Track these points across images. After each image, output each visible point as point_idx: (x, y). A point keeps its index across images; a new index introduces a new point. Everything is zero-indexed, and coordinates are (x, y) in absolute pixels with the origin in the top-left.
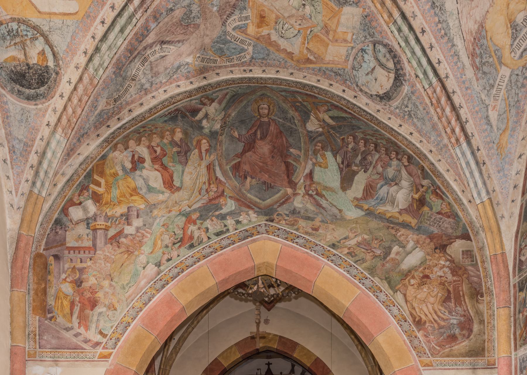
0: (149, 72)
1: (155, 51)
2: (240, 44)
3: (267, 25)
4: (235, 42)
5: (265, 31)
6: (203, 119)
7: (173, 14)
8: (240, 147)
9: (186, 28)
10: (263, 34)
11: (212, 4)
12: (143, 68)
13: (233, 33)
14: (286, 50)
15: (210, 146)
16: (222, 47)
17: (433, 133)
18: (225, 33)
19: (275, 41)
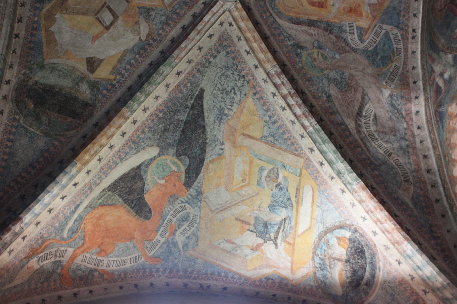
0: (388, 136)
1: (365, 123)
2: (379, 38)
3: (359, 6)
4: (377, 42)
5: (366, 10)
7: (333, 97)
9: (350, 88)
10: (369, 11)
11: (332, 58)
12: (380, 141)
13: (366, 43)
18: (364, 51)
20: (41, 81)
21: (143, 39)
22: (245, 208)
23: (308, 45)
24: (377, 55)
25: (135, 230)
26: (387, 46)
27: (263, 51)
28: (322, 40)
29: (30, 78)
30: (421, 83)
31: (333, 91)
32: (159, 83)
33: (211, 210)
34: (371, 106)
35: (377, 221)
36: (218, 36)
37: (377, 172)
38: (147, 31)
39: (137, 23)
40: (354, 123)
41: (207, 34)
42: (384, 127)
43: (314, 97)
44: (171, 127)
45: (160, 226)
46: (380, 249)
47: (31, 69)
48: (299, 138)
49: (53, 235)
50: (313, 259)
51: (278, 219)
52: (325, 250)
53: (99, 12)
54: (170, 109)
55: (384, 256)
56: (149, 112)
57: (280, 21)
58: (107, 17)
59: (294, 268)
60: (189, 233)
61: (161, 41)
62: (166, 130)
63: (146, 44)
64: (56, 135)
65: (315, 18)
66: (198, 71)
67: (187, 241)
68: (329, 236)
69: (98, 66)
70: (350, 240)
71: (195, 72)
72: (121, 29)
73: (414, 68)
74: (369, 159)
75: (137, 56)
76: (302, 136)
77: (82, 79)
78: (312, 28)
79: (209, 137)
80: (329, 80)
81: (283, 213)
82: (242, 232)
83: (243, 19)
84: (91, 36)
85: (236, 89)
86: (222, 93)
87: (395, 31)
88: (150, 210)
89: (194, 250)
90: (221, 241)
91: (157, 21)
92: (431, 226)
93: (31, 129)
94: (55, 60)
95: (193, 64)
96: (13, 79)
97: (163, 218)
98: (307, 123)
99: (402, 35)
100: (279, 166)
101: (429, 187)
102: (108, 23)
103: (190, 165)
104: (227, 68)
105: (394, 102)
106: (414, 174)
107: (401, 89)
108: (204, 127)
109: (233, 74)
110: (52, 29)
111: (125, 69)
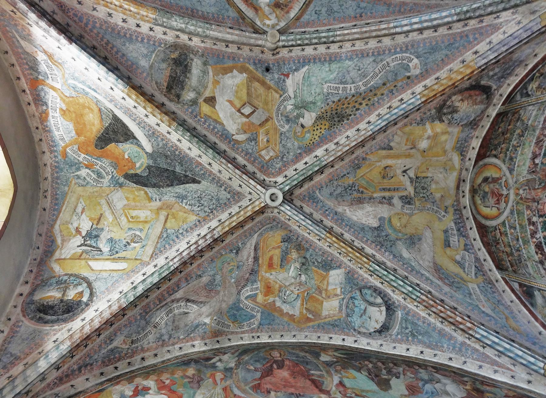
3: (273, 294)
4: (247, 310)
6: (217, 362)
8: (258, 375)
10: (269, 301)
13: (245, 302)
14: (289, 314)
15: (225, 376)
16: (235, 314)
17: (443, 340)
18: (239, 301)
19: (279, 307)
20: (194, 64)
21: (234, 137)
22: (111, 220)
23: (239, 258)
24: (237, 311)
25: (85, 137)
26: (244, 317)
27: (230, 224)
28: (245, 268)
29: (195, 55)
30: (217, 346)
31: (205, 279)
32: (200, 150)
33: (108, 195)
34: (195, 310)
35: (92, 320)
36: (241, 191)
37: (139, 318)
38: (240, 139)
39: (245, 132)
40: (180, 297)
41: (241, 183)
42: (178, 321)
43: (199, 265)
44: (169, 161)
45: (92, 157)
46: (70, 325)
47: (203, 55)
48: (166, 256)
49: (68, 72)
50: (66, 275)
51: (101, 246)
52: (73, 283)
53: (250, 104)
54: (183, 159)
55: (62, 329)
56: (178, 143)
57: (256, 235)
58: (247, 110)
59: (60, 261)
60: (88, 179)
61: (234, 150)
62: (167, 157)
63: (230, 140)
64: (152, 74)
65: (260, 262)
66: (214, 179)
67: (82, 178)
68: (85, 285)
69: (209, 105)
70: (80, 301)
71: (213, 176)
72: (239, 121)
73: (229, 340)
74: (150, 311)
75: (220, 133)
76: (166, 258)
77: (199, 94)
78: (253, 260)
79: (164, 190)
80: (214, 275)
81: (106, 249)
82: (91, 219)
83: (253, 208)
84: (232, 99)
85: (203, 207)
86: (198, 197)
87: (256, 323)
88: (103, 148)
89: (75, 184)
90: (83, 203)
91: (248, 147)
92: (91, 365)
93: (154, 56)
94: (211, 73)
95: (218, 174)
96: (193, 43)
97: (99, 158)
98: (175, 260)
99: (254, 328)
100: (144, 243)
101: (128, 361)
102: (242, 111)
103: (141, 176)
104: (218, 200)
105: (200, 327)
106: (140, 348)
107: (211, 332)
108: (172, 185)
109: (213, 204)
110: (235, 71)
111: (210, 125)
